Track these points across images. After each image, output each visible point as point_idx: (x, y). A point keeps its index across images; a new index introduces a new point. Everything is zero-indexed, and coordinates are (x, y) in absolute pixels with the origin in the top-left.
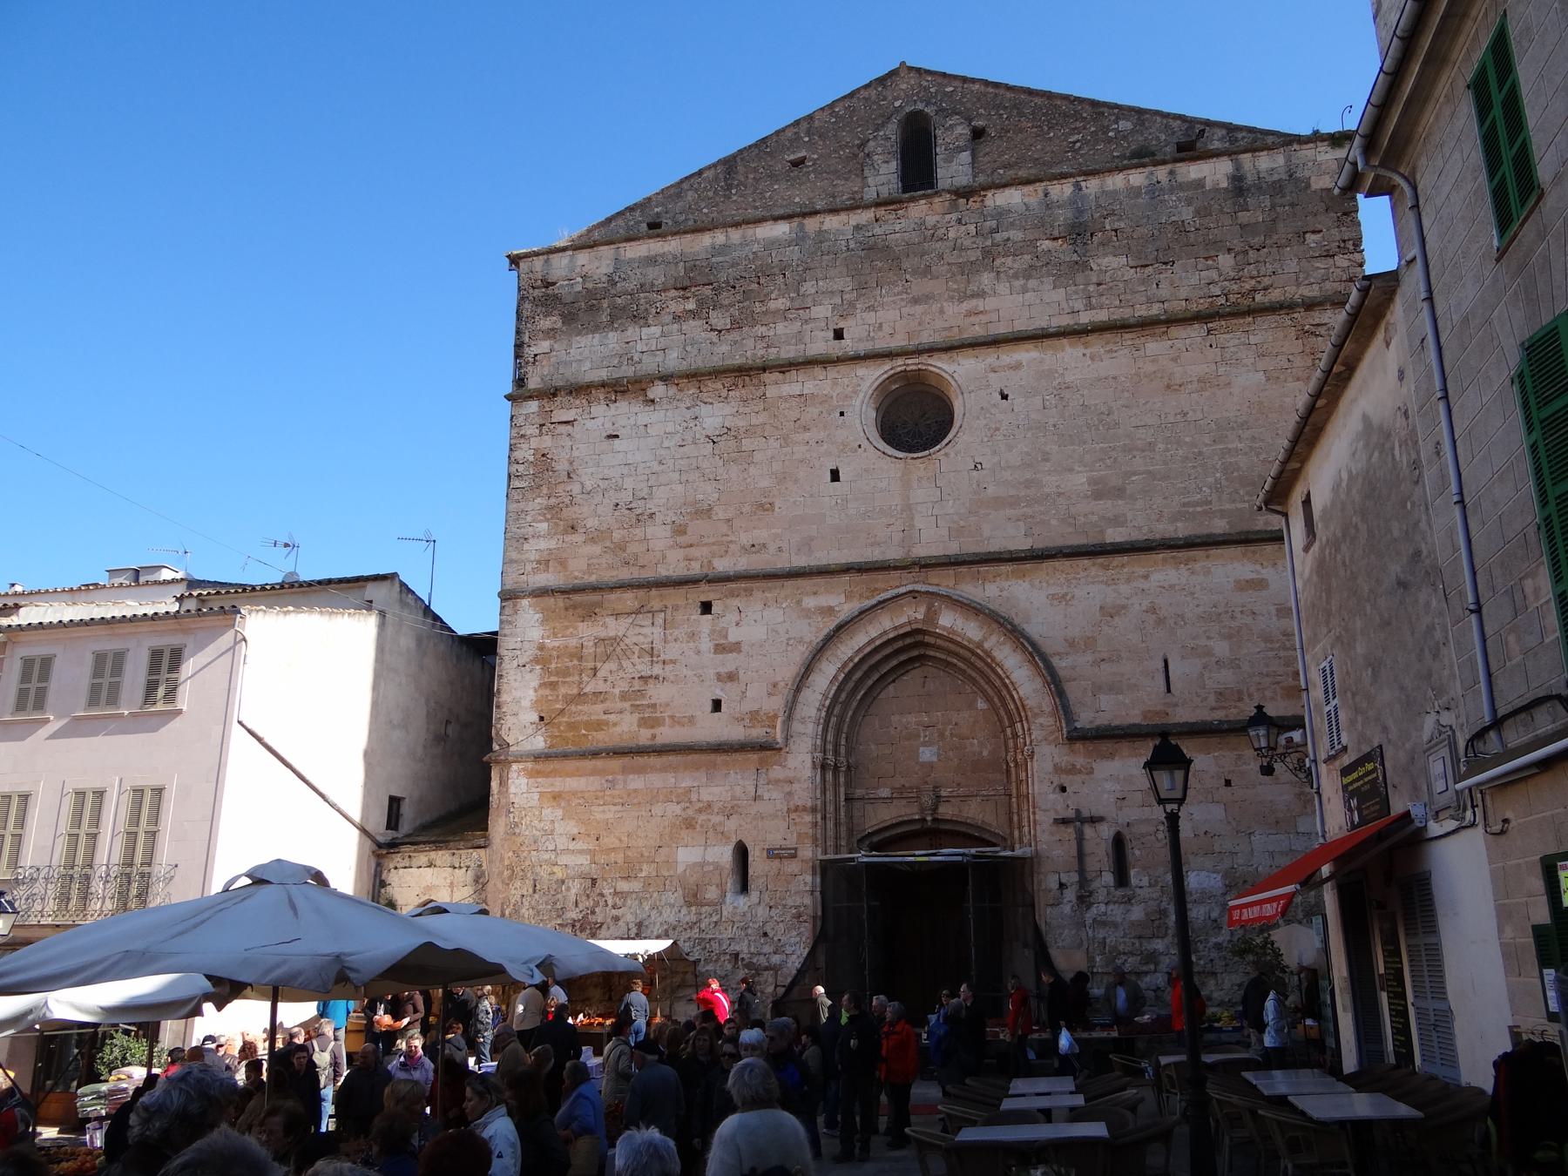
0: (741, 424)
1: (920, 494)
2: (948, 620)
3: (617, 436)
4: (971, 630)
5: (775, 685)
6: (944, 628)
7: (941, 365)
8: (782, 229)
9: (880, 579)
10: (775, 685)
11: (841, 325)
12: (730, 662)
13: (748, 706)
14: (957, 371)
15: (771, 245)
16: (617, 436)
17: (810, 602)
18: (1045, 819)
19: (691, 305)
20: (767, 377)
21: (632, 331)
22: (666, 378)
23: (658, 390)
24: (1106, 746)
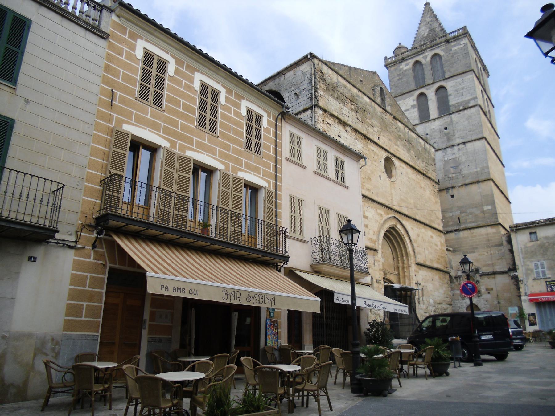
0: (364, 151)
1: (393, 192)
2: (399, 227)
3: (340, 137)
4: (402, 231)
5: (374, 232)
6: (398, 228)
7: (394, 159)
8: (368, 100)
9: (390, 211)
10: (374, 232)
11: (379, 136)
12: (366, 222)
13: (370, 237)
14: (396, 162)
15: (367, 103)
16: (340, 137)
17: (379, 211)
18: (414, 282)
19: (353, 107)
20: (368, 140)
21: (342, 105)
22: (350, 126)
23: (348, 128)
24: (421, 268)
